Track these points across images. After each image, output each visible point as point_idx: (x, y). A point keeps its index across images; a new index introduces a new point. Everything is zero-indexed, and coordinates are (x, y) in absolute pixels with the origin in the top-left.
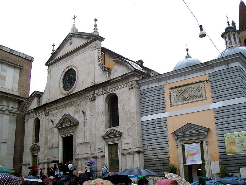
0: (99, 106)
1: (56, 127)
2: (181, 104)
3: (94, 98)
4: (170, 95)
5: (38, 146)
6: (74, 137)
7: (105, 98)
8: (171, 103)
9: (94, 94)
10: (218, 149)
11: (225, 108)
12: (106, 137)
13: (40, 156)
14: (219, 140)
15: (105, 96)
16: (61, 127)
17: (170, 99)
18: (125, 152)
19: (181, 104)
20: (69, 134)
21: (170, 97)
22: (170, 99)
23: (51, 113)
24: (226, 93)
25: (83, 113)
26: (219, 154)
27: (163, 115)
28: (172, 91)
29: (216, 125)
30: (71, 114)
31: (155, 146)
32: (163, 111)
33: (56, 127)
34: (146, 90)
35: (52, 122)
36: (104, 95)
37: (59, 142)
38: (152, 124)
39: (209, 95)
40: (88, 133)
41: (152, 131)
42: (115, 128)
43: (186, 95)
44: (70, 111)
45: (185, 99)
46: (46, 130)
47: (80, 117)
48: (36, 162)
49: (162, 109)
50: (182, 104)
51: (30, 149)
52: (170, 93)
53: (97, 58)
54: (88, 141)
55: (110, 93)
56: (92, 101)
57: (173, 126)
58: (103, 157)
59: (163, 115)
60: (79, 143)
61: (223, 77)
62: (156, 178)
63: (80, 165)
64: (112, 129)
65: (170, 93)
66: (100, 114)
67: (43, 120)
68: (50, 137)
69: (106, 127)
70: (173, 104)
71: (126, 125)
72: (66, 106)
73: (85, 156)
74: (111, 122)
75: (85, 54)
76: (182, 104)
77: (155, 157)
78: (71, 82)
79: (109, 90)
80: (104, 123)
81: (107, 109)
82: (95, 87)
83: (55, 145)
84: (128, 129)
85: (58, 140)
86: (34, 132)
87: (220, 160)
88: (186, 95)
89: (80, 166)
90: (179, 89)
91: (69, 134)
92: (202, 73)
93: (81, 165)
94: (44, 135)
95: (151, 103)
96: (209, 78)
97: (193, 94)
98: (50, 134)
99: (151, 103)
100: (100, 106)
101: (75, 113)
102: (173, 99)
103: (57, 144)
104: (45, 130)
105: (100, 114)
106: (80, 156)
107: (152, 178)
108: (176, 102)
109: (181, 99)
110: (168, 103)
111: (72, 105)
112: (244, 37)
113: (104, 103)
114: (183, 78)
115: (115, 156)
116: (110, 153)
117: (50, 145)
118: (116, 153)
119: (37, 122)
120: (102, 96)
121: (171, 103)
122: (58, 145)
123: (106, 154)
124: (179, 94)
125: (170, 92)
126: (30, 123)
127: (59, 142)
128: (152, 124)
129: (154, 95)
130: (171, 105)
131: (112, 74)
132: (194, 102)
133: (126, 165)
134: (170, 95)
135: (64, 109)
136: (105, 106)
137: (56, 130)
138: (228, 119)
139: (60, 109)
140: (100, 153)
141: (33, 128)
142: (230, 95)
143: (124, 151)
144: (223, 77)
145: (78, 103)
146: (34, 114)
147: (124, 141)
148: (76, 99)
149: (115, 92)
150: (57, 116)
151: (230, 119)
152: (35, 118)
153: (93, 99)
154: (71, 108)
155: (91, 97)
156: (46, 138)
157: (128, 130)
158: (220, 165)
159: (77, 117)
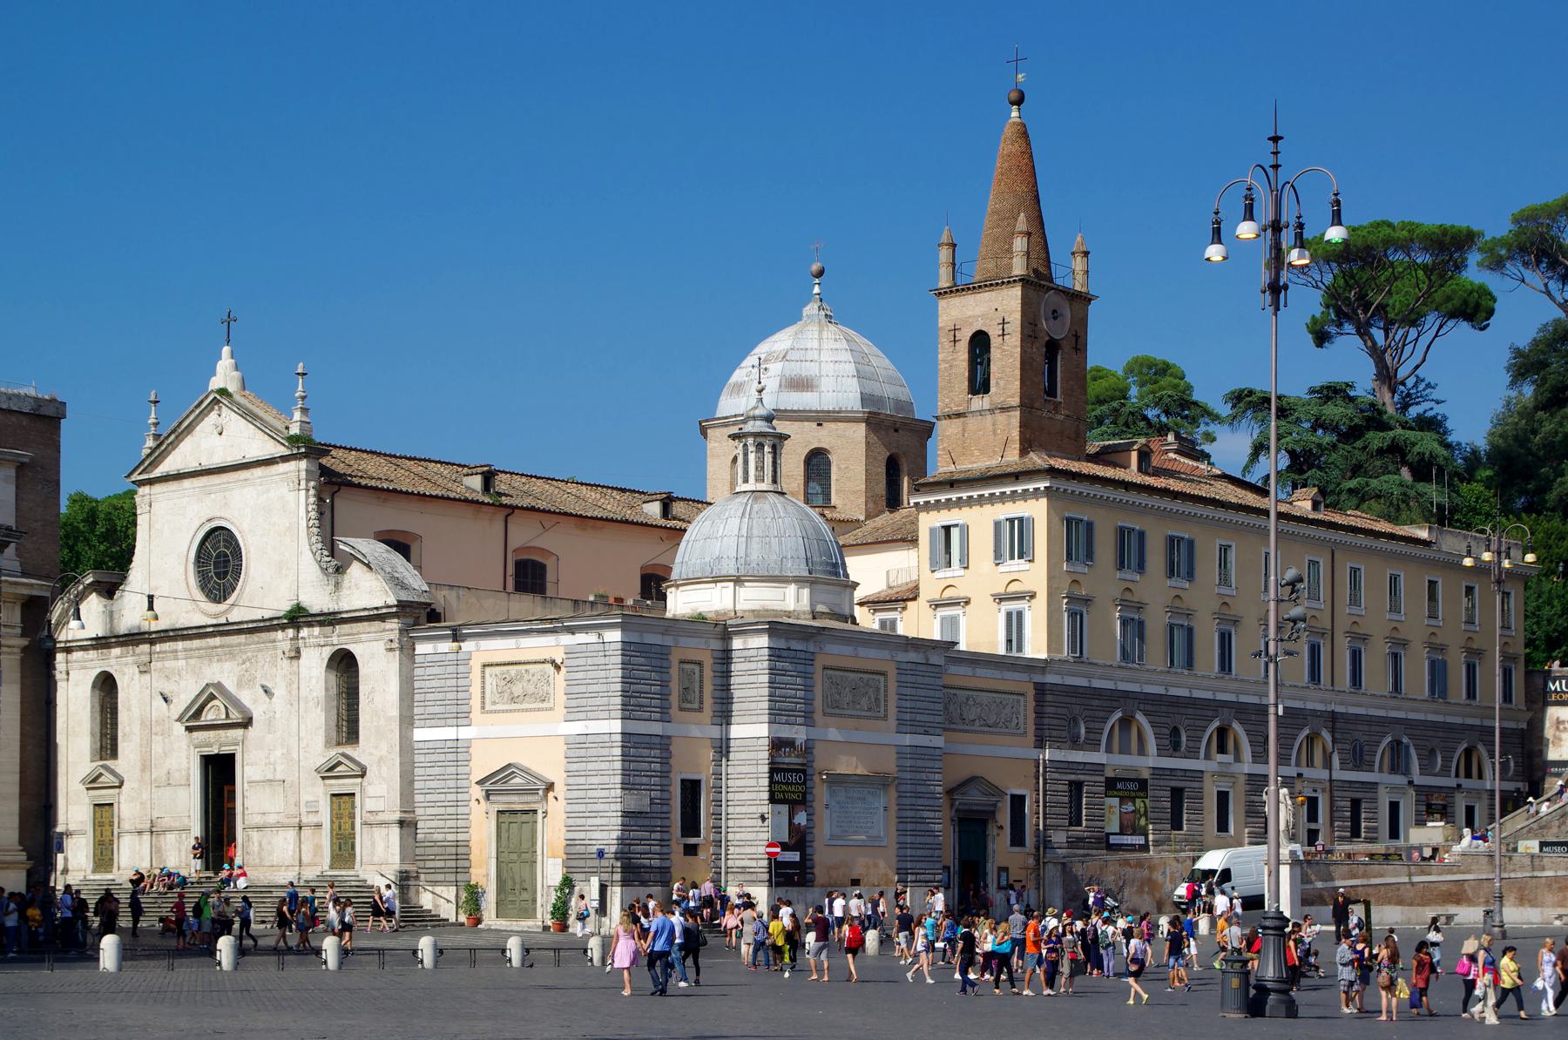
0: (311, 677)
1: (179, 720)
2: (503, 711)
3: (298, 651)
4: (484, 682)
5: (113, 772)
6: (238, 759)
7: (326, 660)
8: (483, 703)
9: (296, 638)
10: (564, 829)
11: (582, 739)
12: (329, 772)
13: (123, 806)
14: (568, 810)
15: (327, 652)
16: (194, 720)
17: (483, 693)
18: (371, 819)
19: (503, 711)
20: (223, 748)
21: (483, 687)
22: (483, 693)
23: (159, 665)
24: (591, 701)
25: (266, 691)
26: (565, 843)
27: (464, 733)
28: (488, 670)
29: (565, 775)
30: (230, 686)
31: (442, 811)
32: (464, 721)
33: (179, 720)
34: (429, 658)
35: (166, 700)
36: (324, 648)
37: (189, 769)
38: (438, 751)
39: (560, 699)
40: (278, 753)
41: (437, 770)
42: (349, 750)
43: (517, 689)
44: (225, 673)
45: (513, 700)
46: (142, 723)
47: (255, 701)
48: (107, 827)
49: (461, 717)
50: (507, 711)
51: (83, 781)
52: (483, 677)
53: (303, 523)
54: (279, 777)
55: (339, 647)
56: (291, 658)
57: (482, 765)
58: (319, 826)
59: (464, 733)
60: (254, 779)
61: (590, 661)
62: (438, 889)
63: (256, 844)
64: (344, 755)
65: (483, 677)
66: (311, 703)
67: (128, 685)
68: (157, 748)
69: (328, 744)
70: (488, 707)
71: (376, 747)
72: (209, 655)
73: (272, 819)
74: (344, 729)
75: (268, 491)
76: (507, 711)
77: (440, 837)
78: (226, 573)
79: (340, 637)
80: (322, 732)
81: (334, 691)
82: (297, 618)
83: (177, 775)
84: (381, 759)
85: (188, 763)
86: (96, 718)
87: (565, 857)
88: (517, 689)
89: (255, 848)
90: (505, 668)
91: (223, 748)
92: (549, 640)
93: (260, 845)
94: (136, 739)
95: (440, 696)
96: (565, 656)
97: (531, 689)
98: (159, 738)
99: (440, 696)
100: (314, 681)
101: (239, 685)
102: (488, 695)
103: (184, 773)
104: (139, 722)
105: (311, 703)
106: (257, 820)
107: (430, 888)
108: (494, 703)
109: (506, 695)
110: (476, 702)
111: (232, 656)
112: (971, 324)
113: (323, 674)
114: (510, 642)
115: (348, 826)
116: (336, 816)
117: (159, 773)
118: (350, 817)
119: (106, 685)
120: (317, 650)
121: (483, 703)
122: (188, 779)
123: (325, 817)
124: (503, 683)
125: (483, 672)
126: (76, 685)
127: (192, 768)
128: (438, 751)
129: (447, 676)
130: (483, 708)
131: (344, 592)
132: (531, 710)
133: (373, 853)
134: (484, 682)
135: (206, 662)
136: (326, 682)
137: (179, 729)
138: (928, 660)
139: (193, 661)
140: (310, 815)
141: (92, 707)
142: (596, 708)
143: (368, 815)
144: (590, 661)
145: (249, 654)
146: (91, 656)
147: (371, 790)
148: (243, 641)
149: (351, 647)
150: (183, 684)
151: (591, 766)
152: (99, 670)
153: (293, 654)
154: (227, 665)
155: (287, 646)
156: (144, 750)
157: (379, 761)
158: (563, 866)
159: (246, 697)
